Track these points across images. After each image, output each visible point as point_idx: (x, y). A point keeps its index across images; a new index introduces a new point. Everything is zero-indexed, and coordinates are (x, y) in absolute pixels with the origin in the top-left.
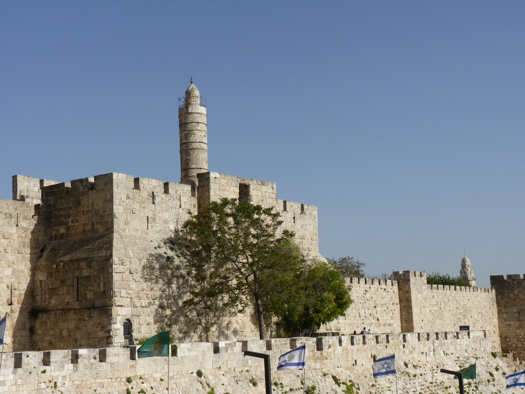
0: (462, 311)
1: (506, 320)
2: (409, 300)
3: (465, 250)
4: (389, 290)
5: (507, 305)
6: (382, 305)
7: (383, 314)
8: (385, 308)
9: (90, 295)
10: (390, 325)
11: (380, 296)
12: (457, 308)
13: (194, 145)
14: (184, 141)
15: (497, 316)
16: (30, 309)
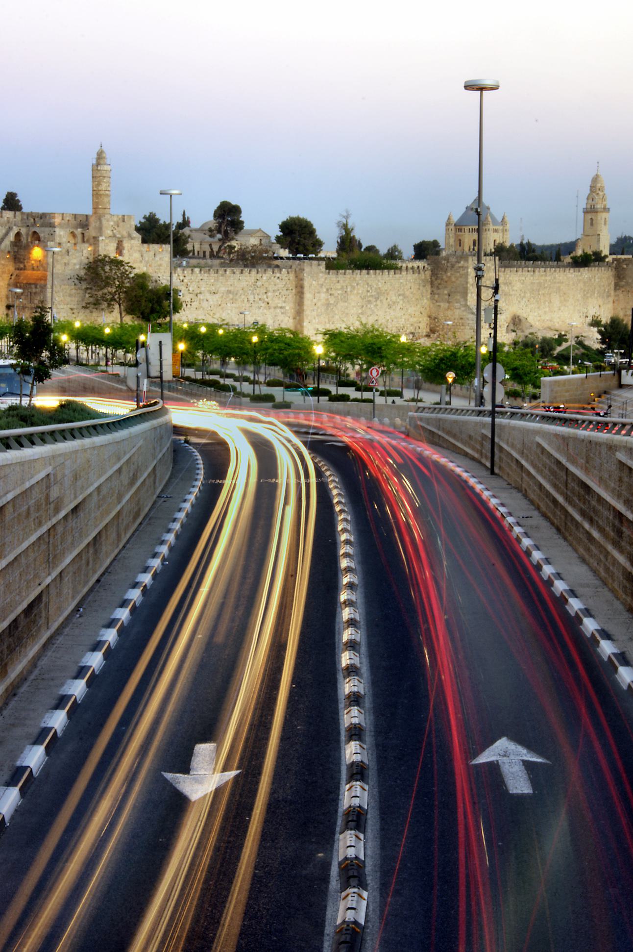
0: (373, 293)
1: (437, 302)
2: (302, 287)
3: (598, 163)
4: (284, 278)
5: (440, 286)
6: (274, 291)
7: (274, 299)
8: (277, 293)
9: (36, 302)
10: (281, 308)
11: (272, 283)
12: (368, 291)
13: (101, 192)
14: (95, 189)
15: (429, 296)
16: (6, 305)
